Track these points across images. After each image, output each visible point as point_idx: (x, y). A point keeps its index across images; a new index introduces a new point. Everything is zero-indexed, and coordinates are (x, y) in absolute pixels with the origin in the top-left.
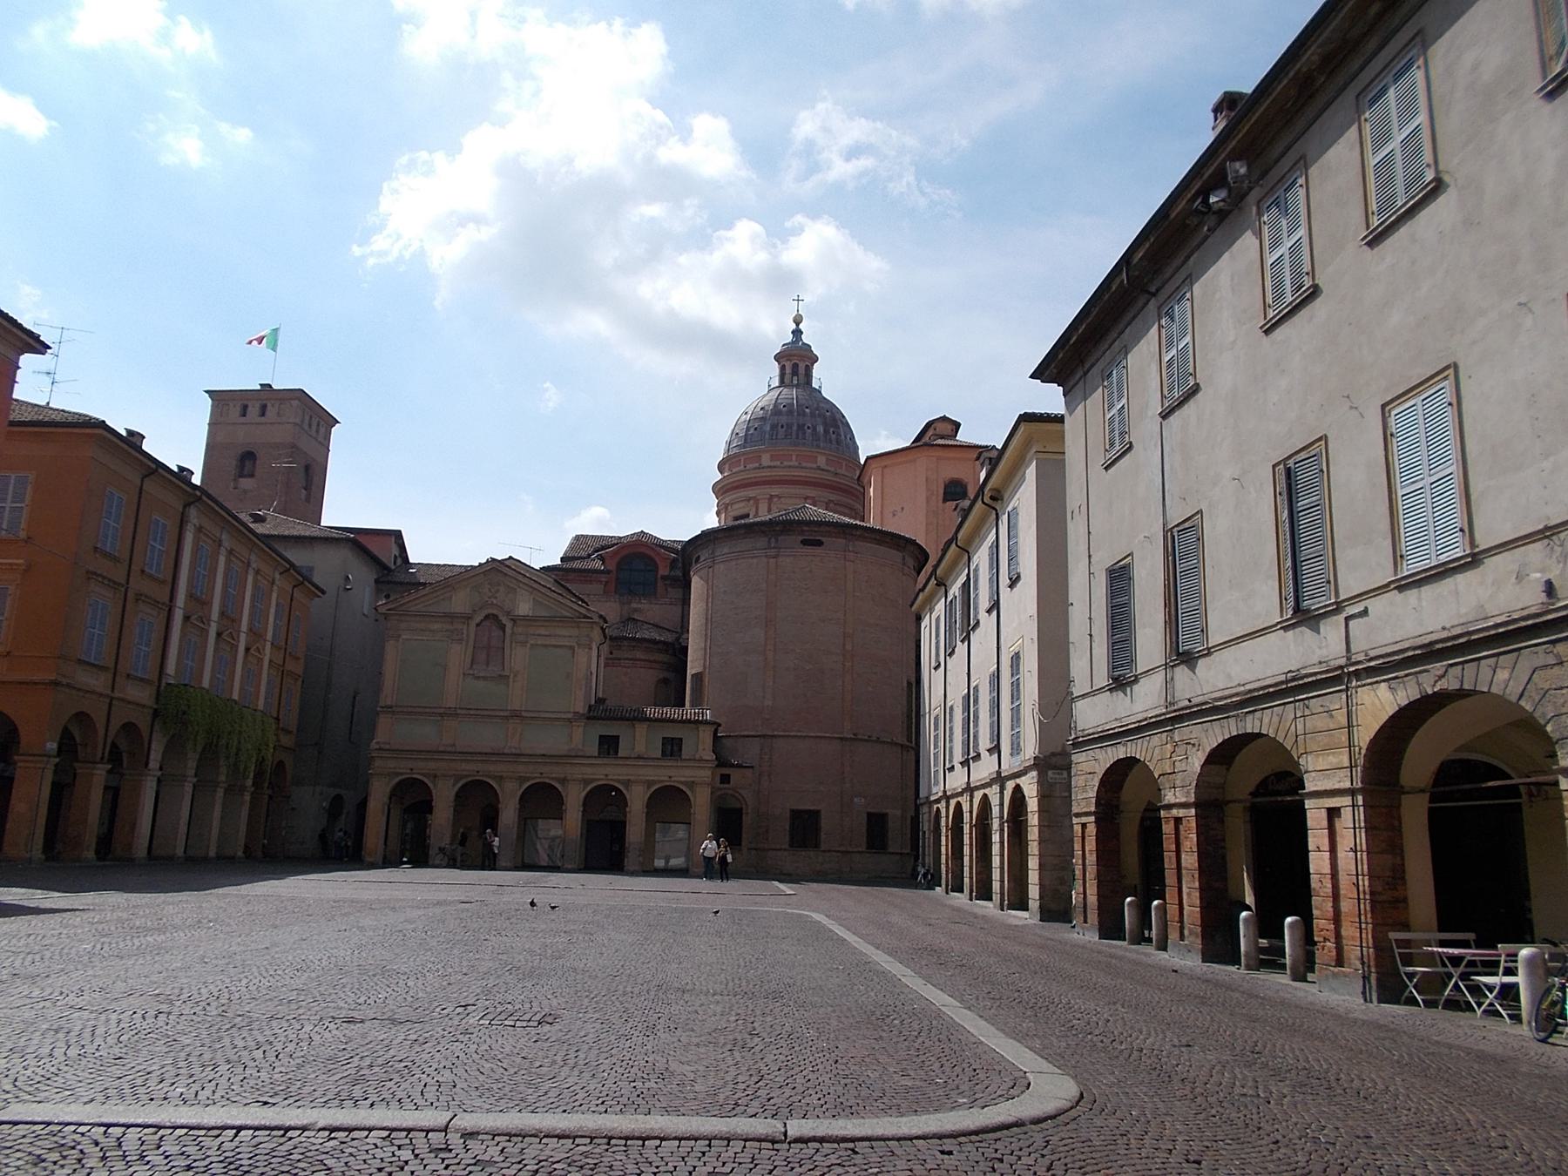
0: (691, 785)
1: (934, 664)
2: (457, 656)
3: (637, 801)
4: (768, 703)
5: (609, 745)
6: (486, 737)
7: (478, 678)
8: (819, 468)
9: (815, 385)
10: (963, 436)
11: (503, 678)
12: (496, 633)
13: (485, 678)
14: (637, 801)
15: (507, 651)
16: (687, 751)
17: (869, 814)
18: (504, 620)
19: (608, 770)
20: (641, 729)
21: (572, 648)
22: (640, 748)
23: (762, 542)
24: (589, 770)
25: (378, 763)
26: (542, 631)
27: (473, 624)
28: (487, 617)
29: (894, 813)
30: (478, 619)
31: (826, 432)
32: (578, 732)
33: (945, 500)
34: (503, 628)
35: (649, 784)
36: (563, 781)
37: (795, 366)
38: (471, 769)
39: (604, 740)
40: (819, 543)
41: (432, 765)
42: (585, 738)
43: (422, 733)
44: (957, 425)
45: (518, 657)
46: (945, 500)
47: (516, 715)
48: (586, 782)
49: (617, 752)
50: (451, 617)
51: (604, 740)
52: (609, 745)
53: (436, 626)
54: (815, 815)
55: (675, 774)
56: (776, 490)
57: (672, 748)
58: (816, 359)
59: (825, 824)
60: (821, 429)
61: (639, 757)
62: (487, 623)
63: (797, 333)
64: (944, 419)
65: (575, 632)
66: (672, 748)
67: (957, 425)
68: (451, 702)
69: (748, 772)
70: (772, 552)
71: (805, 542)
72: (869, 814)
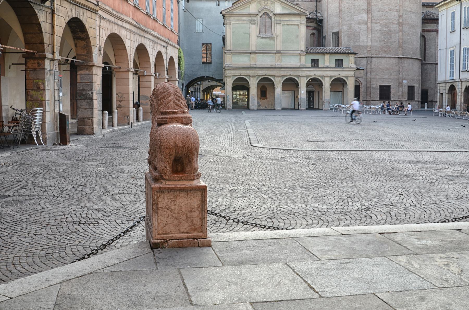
0: (347, 77)
2: (254, 29)
3: (327, 84)
4: (369, 44)
5: (315, 62)
6: (267, 61)
7: (263, 38)
11: (272, 38)
12: (268, 20)
13: (265, 38)
14: (327, 84)
15: (273, 27)
16: (345, 65)
17: (408, 86)
18: (271, 15)
19: (315, 72)
20: (327, 57)
21: (298, 25)
22: (327, 64)
24: (308, 73)
25: (227, 72)
26: (286, 19)
27: (259, 17)
28: (264, 14)
29: (417, 86)
30: (260, 14)
32: (303, 58)
34: (270, 18)
35: (331, 77)
36: (299, 77)
38: (263, 73)
39: (313, 60)
41: (248, 72)
42: (306, 61)
43: (243, 60)
45: (278, 30)
47: (278, 53)
48: (307, 77)
49: (318, 66)
50: (250, 14)
51: (313, 60)
52: (315, 62)
53: (244, 18)
54: (389, 87)
55: (341, 74)
57: (339, 63)
59: (393, 90)
61: (327, 67)
62: (264, 16)
65: (299, 19)
66: (339, 63)
68: (253, 48)
69: (362, 71)
72: (408, 86)
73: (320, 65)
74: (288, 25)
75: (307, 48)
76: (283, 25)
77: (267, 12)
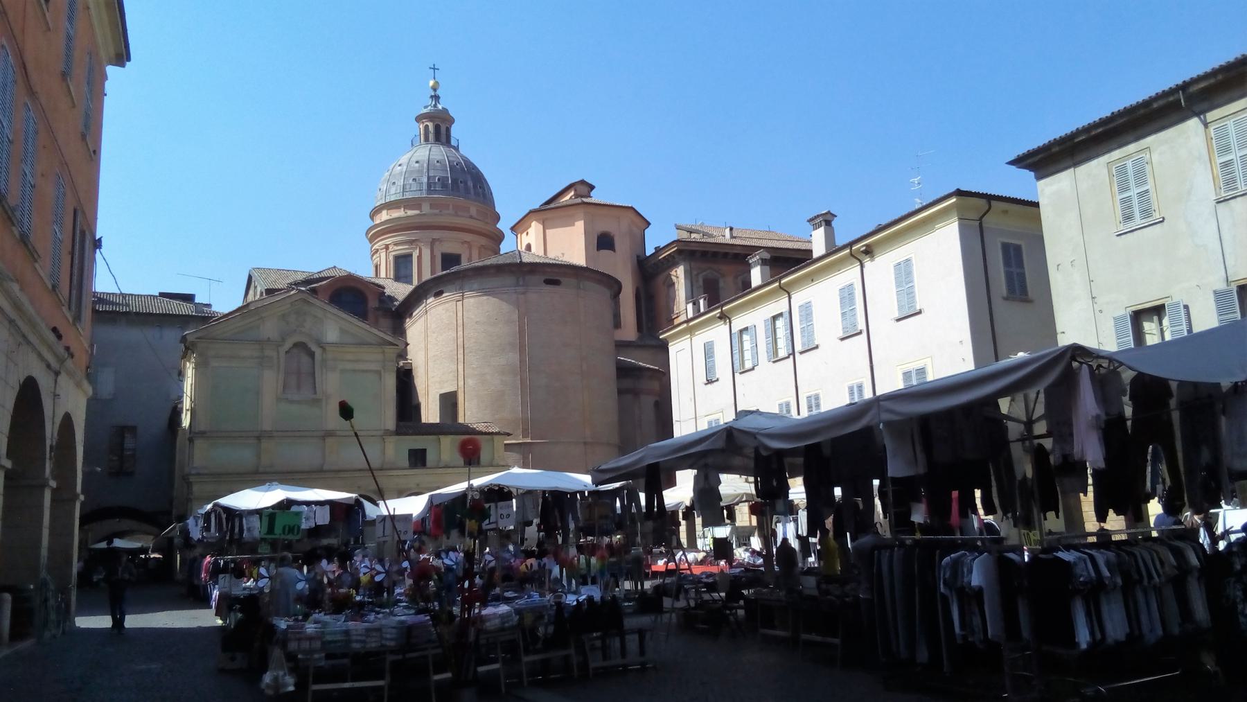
1: (701, 376)
2: (270, 381)
7: (292, 402)
8: (471, 217)
9: (453, 143)
10: (596, 197)
11: (316, 402)
12: (305, 359)
13: (299, 402)
18: (314, 348)
21: (378, 373)
23: (509, 280)
25: (195, 488)
28: (296, 345)
30: (288, 345)
31: (475, 187)
33: (598, 249)
34: (312, 355)
37: (437, 128)
40: (555, 283)
44: (592, 187)
46: (598, 249)
50: (262, 343)
56: (436, 234)
58: (452, 121)
60: (470, 184)
62: (295, 351)
63: (436, 98)
64: (583, 182)
67: (592, 187)
68: (267, 426)
70: (520, 289)
71: (549, 282)
73: (429, 463)
74: (355, 371)
75: (397, 426)
76: (343, 371)
77: (303, 339)
